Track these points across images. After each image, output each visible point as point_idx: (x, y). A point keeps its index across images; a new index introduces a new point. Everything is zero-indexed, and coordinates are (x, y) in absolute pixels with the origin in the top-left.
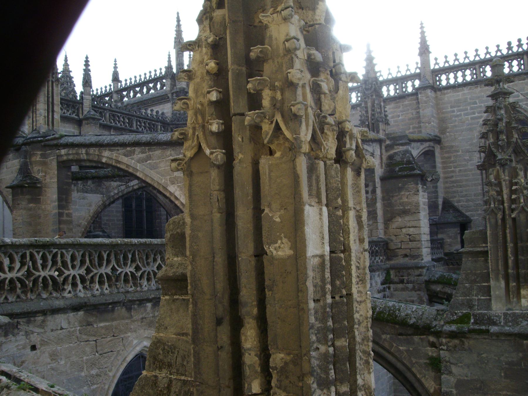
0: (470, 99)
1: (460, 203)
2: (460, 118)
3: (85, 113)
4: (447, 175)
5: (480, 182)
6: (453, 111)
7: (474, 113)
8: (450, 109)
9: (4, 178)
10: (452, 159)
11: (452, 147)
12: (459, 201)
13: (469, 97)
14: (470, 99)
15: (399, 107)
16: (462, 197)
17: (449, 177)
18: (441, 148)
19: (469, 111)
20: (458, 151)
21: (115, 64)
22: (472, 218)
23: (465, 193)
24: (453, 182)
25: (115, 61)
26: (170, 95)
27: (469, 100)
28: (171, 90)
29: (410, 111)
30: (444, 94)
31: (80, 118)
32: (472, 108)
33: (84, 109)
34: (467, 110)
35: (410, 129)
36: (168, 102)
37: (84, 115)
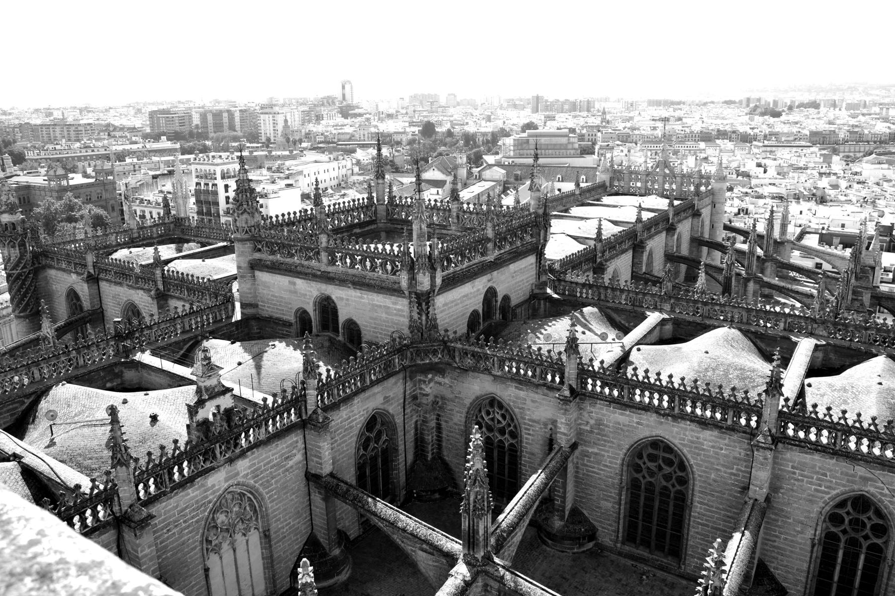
0: (820, 468)
2: (800, 483)
3: (310, 412)
4: (768, 537)
5: (808, 559)
6: (794, 473)
7: (820, 486)
8: (790, 469)
10: (779, 523)
11: (782, 510)
12: (777, 569)
14: (820, 468)
15: (725, 439)
16: (782, 565)
17: (770, 540)
19: (814, 480)
20: (789, 518)
22: (788, 591)
23: (785, 563)
24: (774, 547)
26: (406, 293)
27: (817, 469)
28: (409, 288)
29: (737, 449)
30: (788, 449)
31: (304, 418)
33: (309, 407)
34: (813, 478)
35: (733, 469)
36: (404, 297)
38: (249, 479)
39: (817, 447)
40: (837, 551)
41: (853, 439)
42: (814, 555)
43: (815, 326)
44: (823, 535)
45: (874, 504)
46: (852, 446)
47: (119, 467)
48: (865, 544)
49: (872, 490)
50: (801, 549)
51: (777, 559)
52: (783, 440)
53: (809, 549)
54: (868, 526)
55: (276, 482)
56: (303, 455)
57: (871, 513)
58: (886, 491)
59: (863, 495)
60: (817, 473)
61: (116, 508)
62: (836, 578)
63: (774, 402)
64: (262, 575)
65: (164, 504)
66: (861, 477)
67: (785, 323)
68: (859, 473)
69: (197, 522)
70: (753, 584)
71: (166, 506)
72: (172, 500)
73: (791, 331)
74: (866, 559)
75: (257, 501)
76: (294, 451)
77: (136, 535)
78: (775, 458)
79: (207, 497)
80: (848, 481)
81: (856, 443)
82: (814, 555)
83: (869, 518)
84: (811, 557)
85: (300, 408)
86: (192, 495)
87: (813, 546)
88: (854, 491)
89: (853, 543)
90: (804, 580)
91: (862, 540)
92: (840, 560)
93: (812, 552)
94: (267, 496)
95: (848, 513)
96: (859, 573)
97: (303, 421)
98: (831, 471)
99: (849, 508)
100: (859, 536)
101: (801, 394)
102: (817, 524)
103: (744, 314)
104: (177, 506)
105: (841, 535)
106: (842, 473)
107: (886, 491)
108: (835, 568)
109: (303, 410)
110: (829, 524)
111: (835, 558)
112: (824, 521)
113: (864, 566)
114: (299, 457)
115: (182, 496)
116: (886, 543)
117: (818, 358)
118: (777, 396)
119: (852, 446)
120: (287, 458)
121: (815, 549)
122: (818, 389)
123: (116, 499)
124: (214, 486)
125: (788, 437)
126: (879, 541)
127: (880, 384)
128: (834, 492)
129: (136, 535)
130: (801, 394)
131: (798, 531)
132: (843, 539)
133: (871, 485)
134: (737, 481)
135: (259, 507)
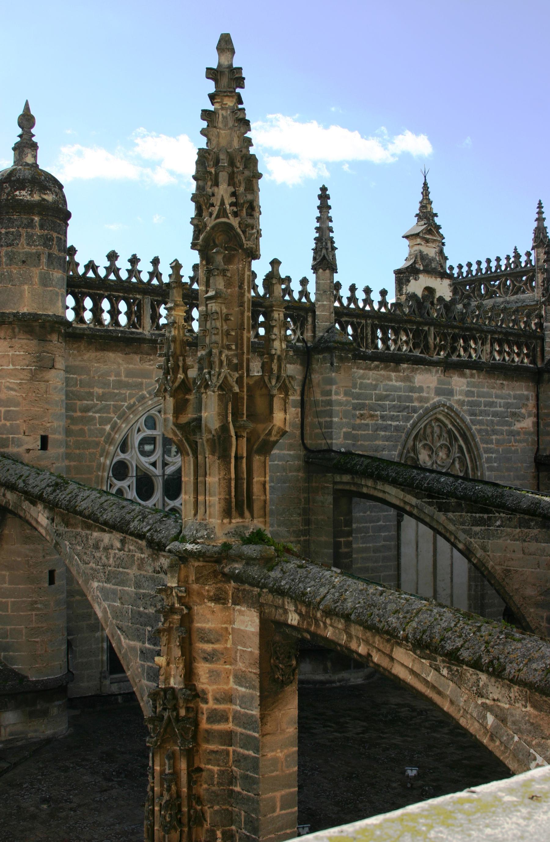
9: (516, 571)
21: (540, 213)
25: (540, 206)
31: (539, 366)
37: (546, 361)
38: (464, 411)
47: (321, 271)
55: (498, 442)
56: (533, 423)
61: (308, 335)
64: (465, 588)
65: (362, 371)
69: (397, 429)
71: (362, 377)
72: (371, 373)
75: (470, 457)
76: (523, 411)
77: (332, 364)
79: (411, 400)
85: (534, 349)
86: (394, 383)
94: (485, 456)
97: (538, 368)
104: (375, 387)
109: (539, 353)
114: (528, 423)
115: (383, 376)
120: (514, 414)
123: (310, 320)
124: (421, 389)
129: (332, 364)
135: (473, 469)
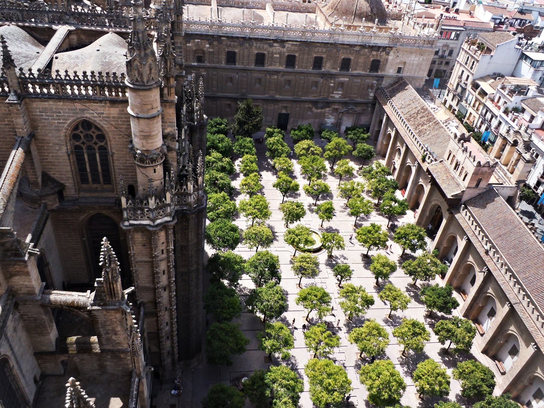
0: (55, 109)
1: (56, 176)
5: (69, 164)
6: (42, 115)
8: (39, 114)
10: (46, 148)
11: (44, 140)
12: (55, 174)
13: (54, 107)
14: (55, 109)
17: (44, 159)
18: (35, 140)
19: (55, 117)
20: (50, 143)
23: (57, 170)
24: (48, 162)
32: (57, 116)
34: (53, 116)
35: (5, 121)
39: (50, 97)
40: (83, 155)
41: (68, 87)
42: (72, 161)
43: (67, 17)
44: (73, 148)
45: (93, 124)
46: (69, 91)
48: (96, 147)
49: (88, 115)
50: (63, 159)
51: (52, 168)
52: (28, 96)
53: (67, 158)
54: (94, 137)
57: (93, 129)
58: (96, 115)
59: (85, 120)
60: (55, 112)
62: (88, 170)
63: (11, 72)
66: (80, 109)
67: (48, 17)
68: (78, 107)
70: (42, 186)
73: (54, 23)
74: (100, 155)
78: (27, 108)
80: (74, 113)
81: (71, 89)
82: (72, 161)
83: (94, 132)
84: (70, 163)
87: (69, 155)
88: (79, 119)
89: (89, 148)
90: (71, 176)
91: (94, 145)
92: (87, 160)
93: (69, 159)
95: (81, 132)
96: (99, 164)
98: (62, 109)
99: (81, 129)
100: (91, 143)
101: (49, 65)
102: (66, 143)
103: (19, 14)
105: (82, 145)
106: (69, 109)
107: (96, 115)
108: (86, 165)
110: (73, 141)
111: (84, 159)
112: (70, 140)
113: (101, 160)
116: (106, 143)
117: (74, 39)
118: (12, 68)
119: (69, 91)
121: (71, 157)
122: (62, 60)
125: (30, 94)
126: (102, 144)
127: (98, 50)
128: (69, 122)
130: (49, 65)
131: (57, 150)
132: (84, 147)
133: (87, 113)
134: (11, 128)
